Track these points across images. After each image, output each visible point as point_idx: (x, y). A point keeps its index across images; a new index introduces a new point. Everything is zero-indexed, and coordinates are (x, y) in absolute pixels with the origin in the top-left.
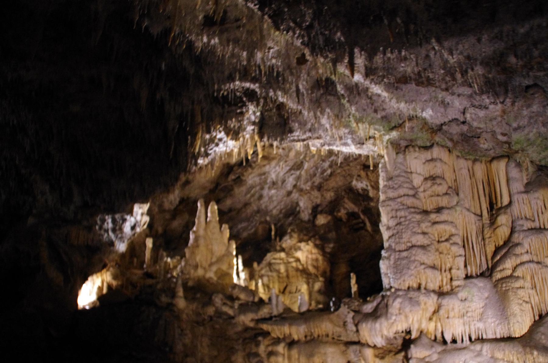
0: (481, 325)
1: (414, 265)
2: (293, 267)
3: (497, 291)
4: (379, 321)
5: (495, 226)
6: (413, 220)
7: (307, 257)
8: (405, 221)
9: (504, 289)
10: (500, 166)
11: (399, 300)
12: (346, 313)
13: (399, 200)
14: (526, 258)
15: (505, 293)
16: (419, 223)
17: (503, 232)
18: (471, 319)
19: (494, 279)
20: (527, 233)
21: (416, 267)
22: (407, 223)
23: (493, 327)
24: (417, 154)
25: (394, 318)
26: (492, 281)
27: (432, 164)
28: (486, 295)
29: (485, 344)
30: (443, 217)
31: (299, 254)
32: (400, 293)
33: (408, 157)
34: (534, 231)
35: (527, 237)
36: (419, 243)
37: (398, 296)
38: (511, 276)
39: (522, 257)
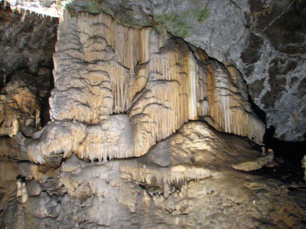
0: (116, 149)
1: (70, 102)
2: (10, 106)
4: (40, 144)
5: (138, 76)
6: (74, 67)
7: (22, 99)
8: (68, 69)
9: (135, 122)
10: (146, 34)
11: (55, 128)
13: (66, 52)
14: (152, 100)
16: (78, 70)
17: (142, 82)
18: (110, 144)
19: (131, 116)
20: (155, 83)
21: (70, 104)
22: (69, 70)
23: (123, 151)
24: (86, 18)
25: (50, 141)
26: (129, 116)
27: (96, 27)
28: (123, 127)
29: (116, 161)
30: (99, 67)
31: (17, 97)
32: (57, 123)
33: (79, 20)
34: (160, 82)
35: (155, 85)
36: (76, 86)
37: (55, 125)
39: (149, 100)
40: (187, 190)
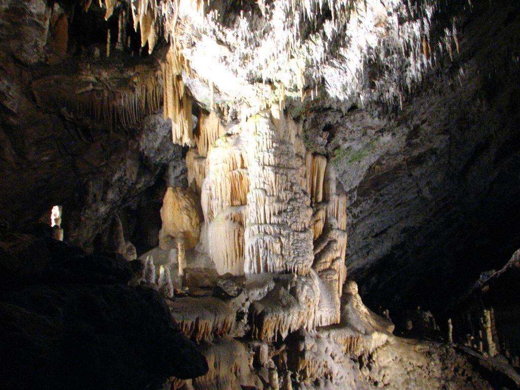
3: (323, 282)
5: (316, 219)
9: (329, 280)
12: (244, 301)
15: (330, 285)
19: (318, 270)
37: (304, 284)
38: (330, 269)
40: (377, 359)
